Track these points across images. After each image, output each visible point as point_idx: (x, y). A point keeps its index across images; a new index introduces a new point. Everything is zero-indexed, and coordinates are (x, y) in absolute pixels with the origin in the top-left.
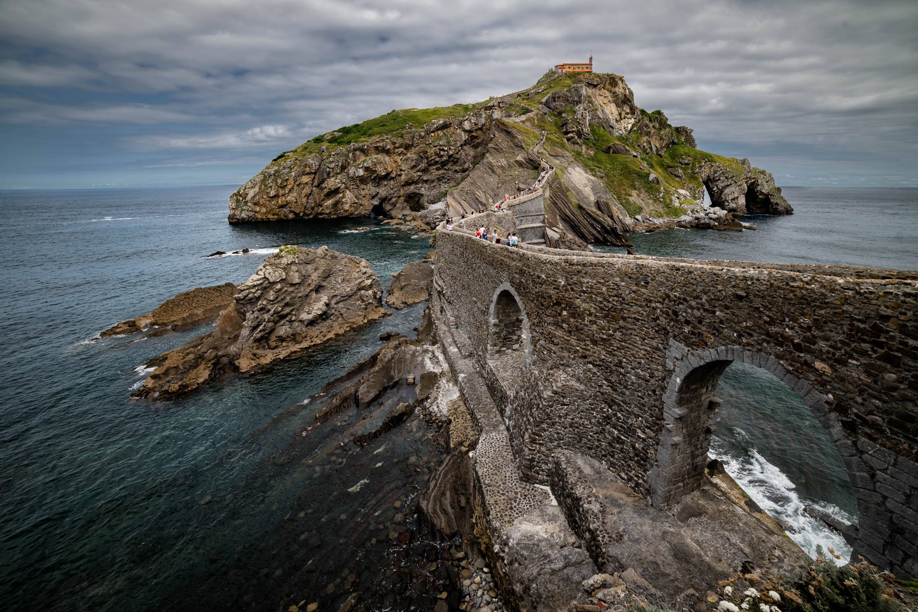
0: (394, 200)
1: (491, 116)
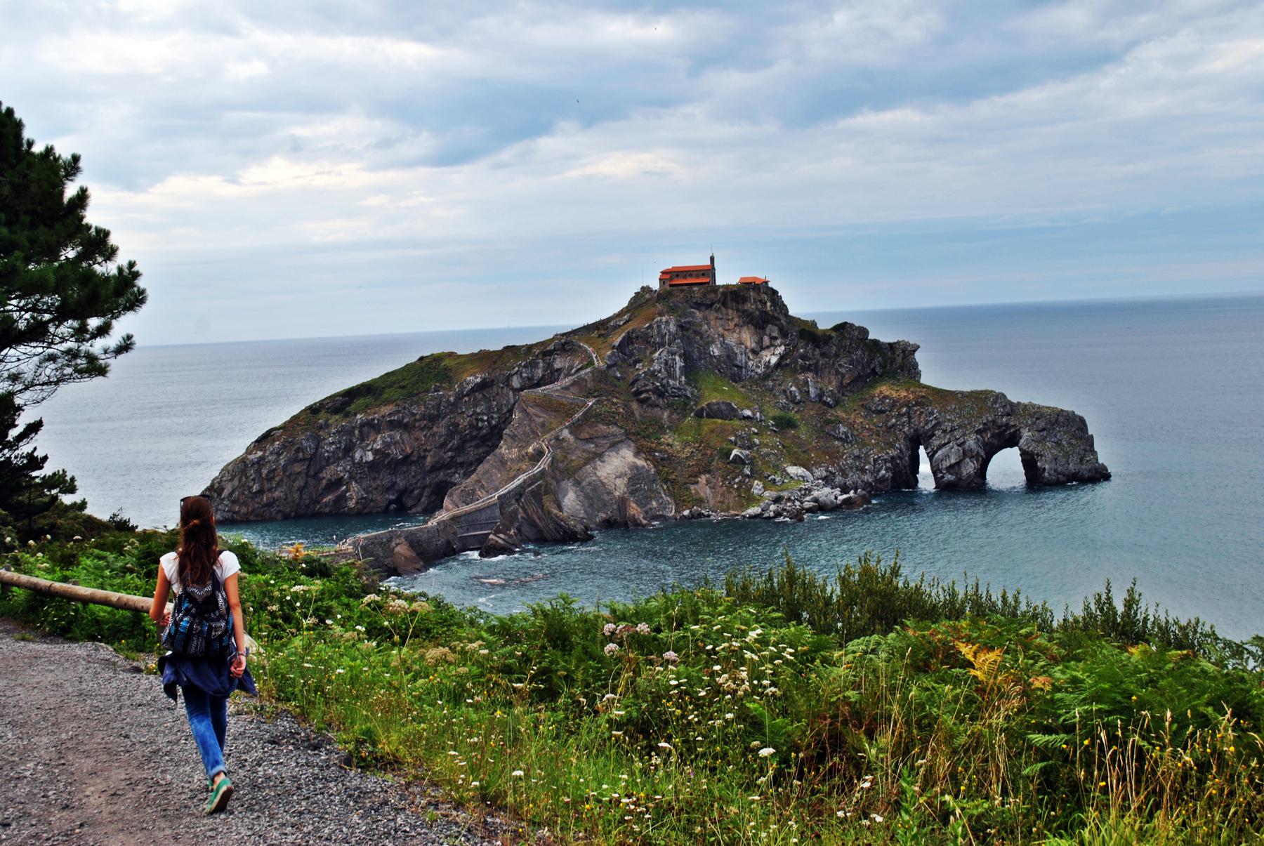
0: (416, 492)
1: (550, 365)
